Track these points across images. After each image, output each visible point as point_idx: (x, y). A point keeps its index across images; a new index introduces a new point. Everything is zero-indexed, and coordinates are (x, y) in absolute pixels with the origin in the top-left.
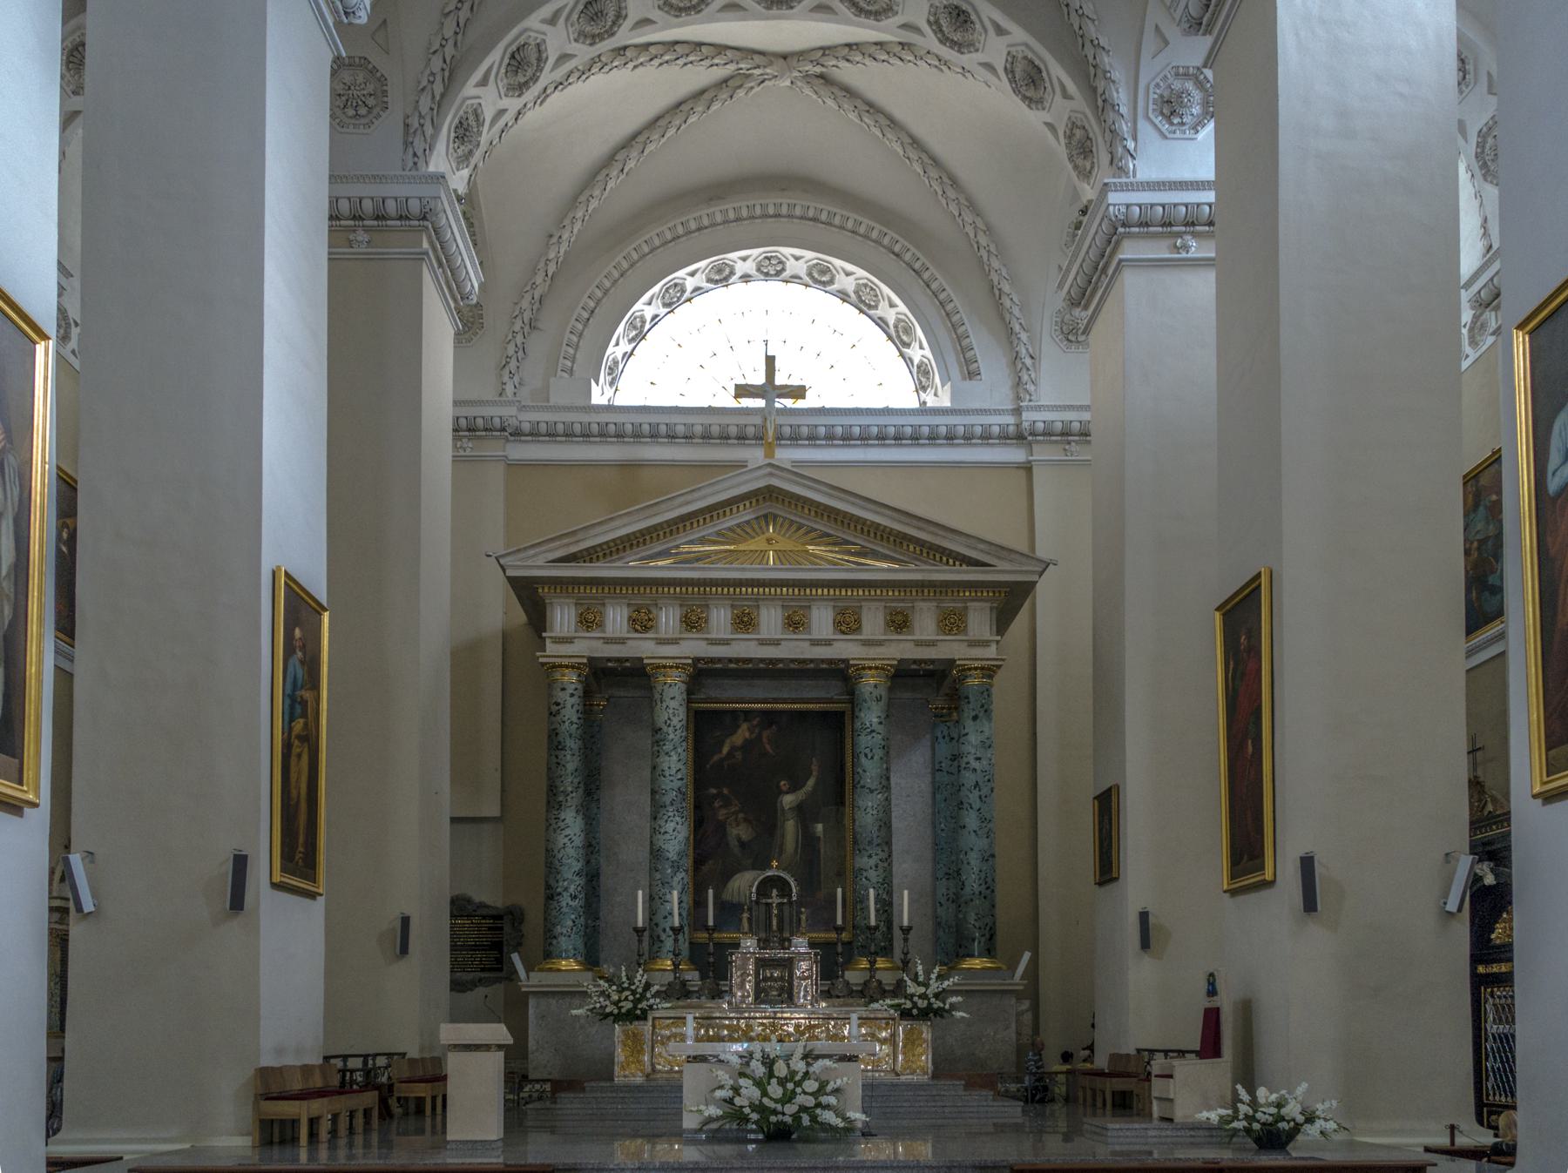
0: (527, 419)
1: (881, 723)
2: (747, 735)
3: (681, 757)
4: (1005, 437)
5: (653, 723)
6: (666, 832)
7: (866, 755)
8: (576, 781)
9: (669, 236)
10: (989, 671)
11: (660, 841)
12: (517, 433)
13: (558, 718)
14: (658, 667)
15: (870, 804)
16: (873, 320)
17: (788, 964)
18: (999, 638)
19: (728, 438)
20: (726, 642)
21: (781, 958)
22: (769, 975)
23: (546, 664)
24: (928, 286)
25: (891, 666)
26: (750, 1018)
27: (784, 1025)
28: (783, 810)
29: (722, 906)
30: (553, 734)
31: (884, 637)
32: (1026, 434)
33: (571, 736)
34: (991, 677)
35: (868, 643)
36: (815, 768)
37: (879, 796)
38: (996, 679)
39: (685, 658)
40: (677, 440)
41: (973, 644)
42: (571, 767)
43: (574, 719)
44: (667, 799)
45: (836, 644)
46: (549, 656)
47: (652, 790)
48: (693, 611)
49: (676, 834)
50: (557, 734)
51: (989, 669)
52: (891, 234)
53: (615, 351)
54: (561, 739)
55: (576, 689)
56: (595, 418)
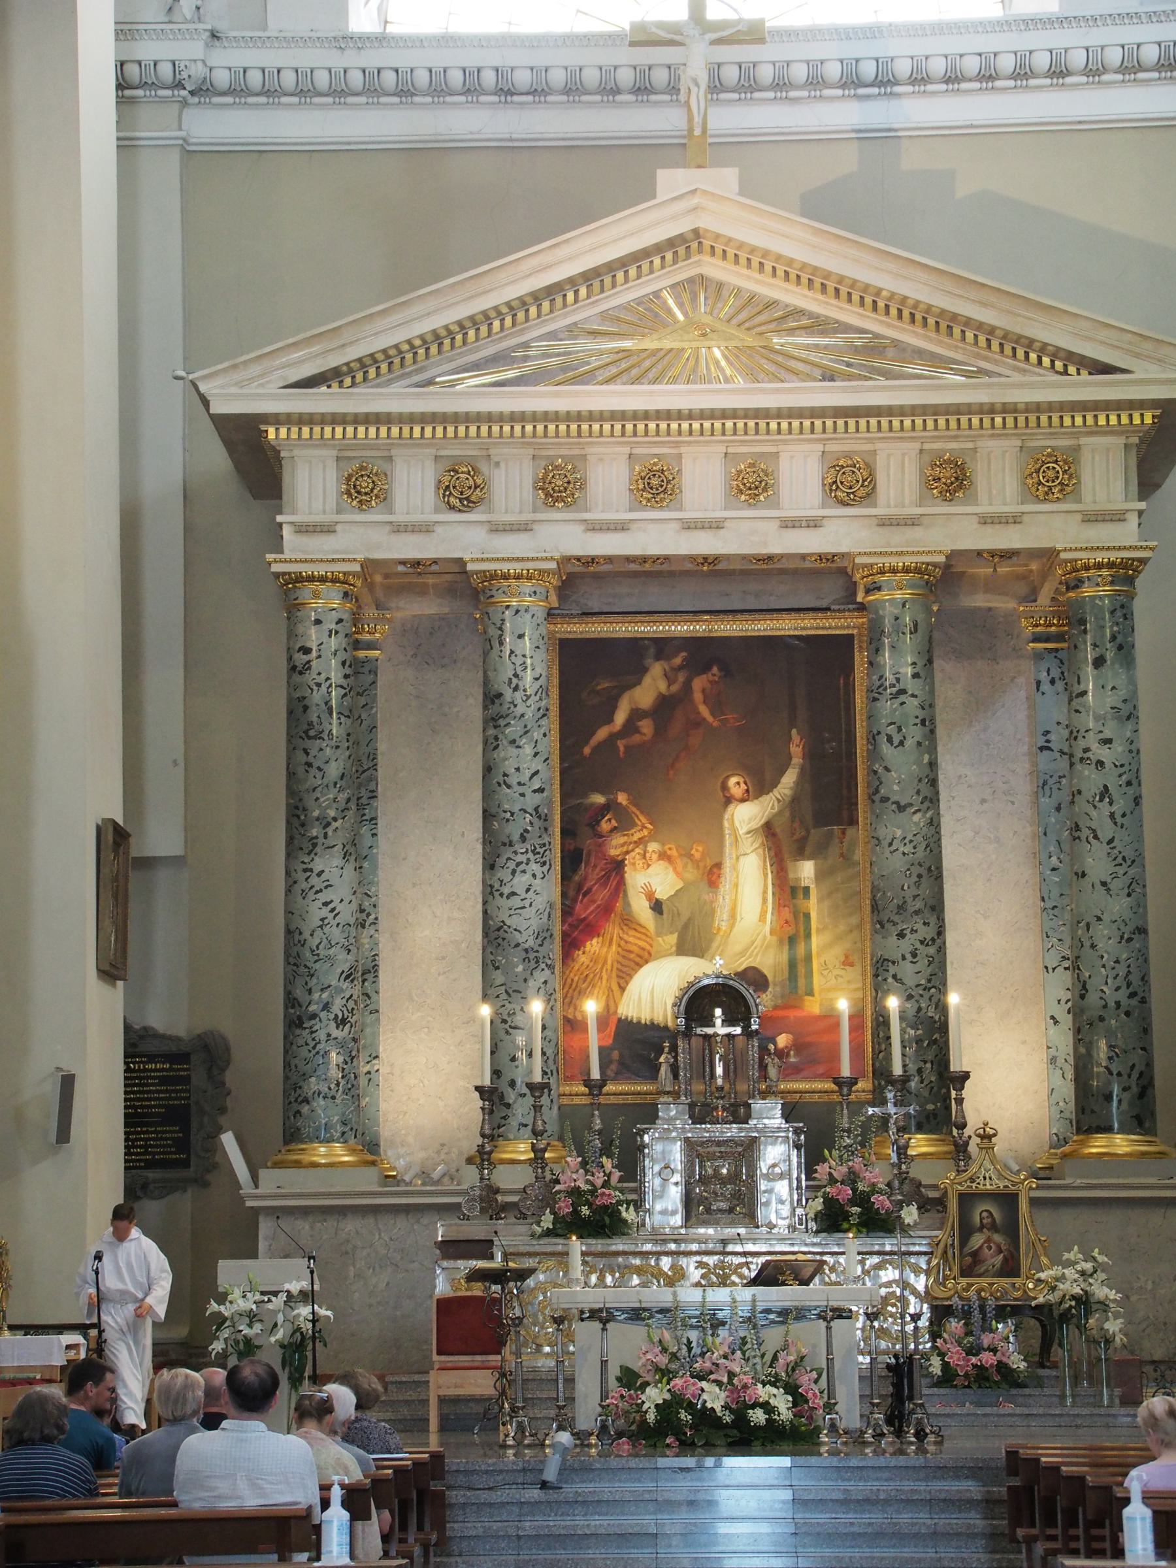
1: (915, 676)
2: (662, 686)
3: (540, 748)
6: (514, 894)
7: (890, 739)
8: (342, 797)
11: (503, 910)
12: (204, 90)
14: (493, 576)
15: (899, 833)
17: (748, 1150)
18: (1142, 505)
19: (616, 91)
20: (621, 527)
22: (710, 1171)
23: (284, 574)
25: (935, 565)
27: (740, 1266)
28: (734, 830)
31: (919, 511)
34: (1130, 581)
35: (885, 522)
37: (916, 818)
39: (546, 559)
40: (516, 98)
41: (1093, 518)
42: (334, 770)
45: (830, 527)
46: (291, 561)
47: (485, 811)
48: (557, 467)
50: (306, 708)
51: (1125, 564)
55: (340, 621)
56: (353, 60)
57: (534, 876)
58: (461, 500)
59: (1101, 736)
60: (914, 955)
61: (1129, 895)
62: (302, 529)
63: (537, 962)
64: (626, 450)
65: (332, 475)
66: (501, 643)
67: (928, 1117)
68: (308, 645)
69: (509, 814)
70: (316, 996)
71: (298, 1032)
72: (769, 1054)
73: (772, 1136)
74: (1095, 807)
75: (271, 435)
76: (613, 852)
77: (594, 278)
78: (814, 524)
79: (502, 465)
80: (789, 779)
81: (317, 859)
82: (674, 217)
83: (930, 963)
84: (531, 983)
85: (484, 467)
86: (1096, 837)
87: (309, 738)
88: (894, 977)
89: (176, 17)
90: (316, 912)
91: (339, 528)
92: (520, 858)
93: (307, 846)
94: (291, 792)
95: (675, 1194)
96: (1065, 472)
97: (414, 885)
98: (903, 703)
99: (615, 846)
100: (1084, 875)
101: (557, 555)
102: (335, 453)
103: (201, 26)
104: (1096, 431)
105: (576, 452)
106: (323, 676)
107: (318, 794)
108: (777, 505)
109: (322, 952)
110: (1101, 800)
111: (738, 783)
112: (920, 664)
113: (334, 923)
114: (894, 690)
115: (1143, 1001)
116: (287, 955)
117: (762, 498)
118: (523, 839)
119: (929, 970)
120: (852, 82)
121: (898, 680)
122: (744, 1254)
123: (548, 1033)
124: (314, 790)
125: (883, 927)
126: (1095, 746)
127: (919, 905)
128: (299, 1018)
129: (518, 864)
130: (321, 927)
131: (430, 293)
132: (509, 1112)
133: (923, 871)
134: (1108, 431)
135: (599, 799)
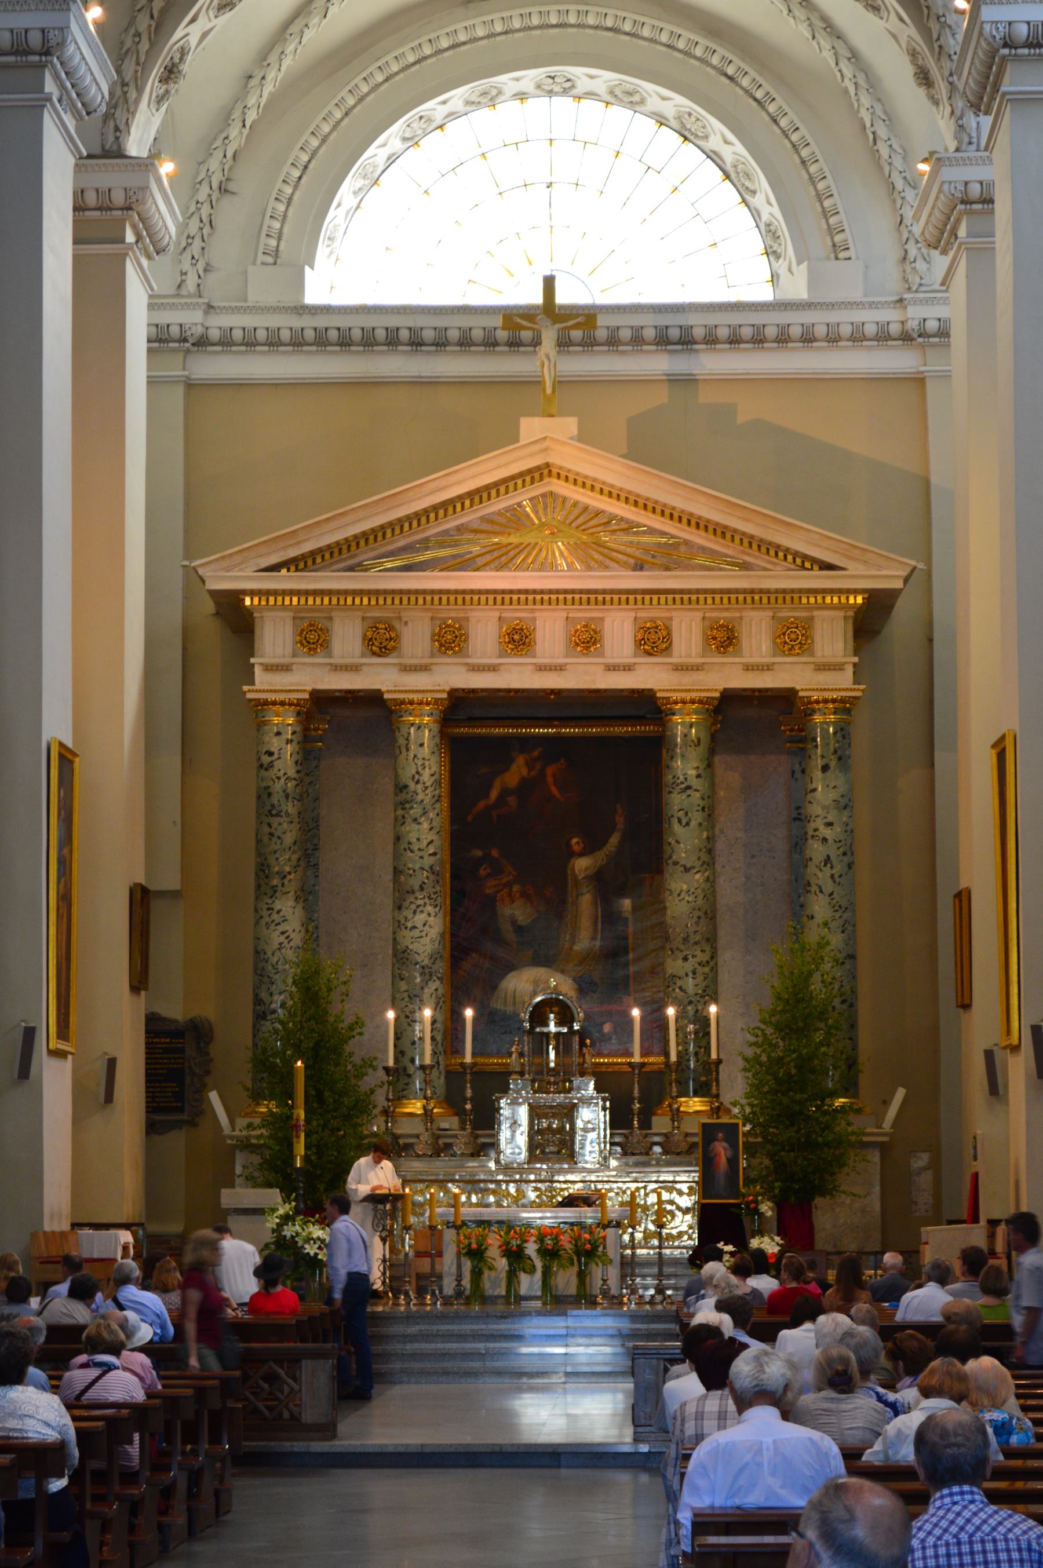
0: (218, 323)
1: (698, 776)
2: (524, 771)
3: (434, 824)
4: (883, 337)
5: (396, 776)
6: (414, 927)
7: (680, 821)
8: (295, 857)
11: (406, 938)
13: (272, 773)
14: (403, 702)
15: (685, 887)
16: (704, 152)
17: (569, 1112)
20: (493, 668)
21: (559, 1105)
23: (254, 700)
24: (775, 121)
25: (713, 698)
26: (521, 1181)
28: (575, 877)
29: (487, 1018)
30: (264, 794)
31: (703, 660)
32: (915, 335)
33: (287, 796)
34: (848, 711)
35: (679, 668)
36: (620, 821)
37: (697, 876)
40: (424, 348)
41: (821, 667)
42: (289, 839)
43: (292, 772)
46: (260, 691)
47: (395, 868)
48: (448, 626)
50: (270, 795)
52: (721, 51)
54: (274, 800)
57: (429, 915)
58: (380, 648)
59: (826, 820)
60: (694, 973)
61: (843, 932)
62: (269, 668)
63: (431, 975)
64: (497, 614)
65: (289, 629)
66: (407, 750)
67: (701, 1086)
68: (272, 749)
69: (411, 872)
70: (275, 997)
71: (263, 1022)
72: (586, 1046)
73: (587, 1102)
74: (821, 870)
75: (248, 602)
76: (488, 891)
77: (477, 495)
78: (628, 668)
79: (410, 624)
80: (614, 840)
81: (277, 901)
82: (531, 455)
83: (705, 978)
84: (426, 990)
85: (397, 625)
86: (821, 891)
87: (272, 816)
88: (680, 988)
89: (183, 292)
90: (276, 939)
91: (294, 667)
92: (419, 902)
93: (270, 892)
94: (259, 854)
95: (522, 1140)
96: (803, 635)
97: (345, 912)
98: (689, 796)
99: (490, 887)
100: (812, 917)
101: (447, 689)
102: (292, 614)
103: (200, 300)
105: (462, 615)
106: (282, 772)
107: (277, 855)
108: (602, 654)
109: (280, 967)
110: (825, 865)
111: (578, 843)
112: (702, 767)
113: (288, 946)
114: (683, 786)
115: (851, 1005)
116: (256, 969)
117: (592, 649)
118: (422, 889)
119: (705, 983)
120: (663, 340)
121: (686, 779)
122: (565, 1182)
123: (436, 1025)
124: (275, 852)
125: (673, 952)
126: (821, 828)
127: (698, 938)
128: (264, 1013)
129: (418, 906)
130: (279, 949)
131: (360, 507)
132: (410, 1080)
133: (701, 914)
134: (832, 607)
135: (479, 853)
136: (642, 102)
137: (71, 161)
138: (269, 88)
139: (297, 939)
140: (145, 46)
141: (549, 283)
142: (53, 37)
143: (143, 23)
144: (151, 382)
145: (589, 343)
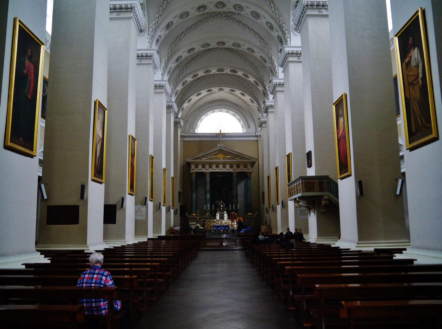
0: (187, 135)
4: (254, 136)
9: (206, 108)
10: (251, 173)
12: (185, 137)
17: (223, 215)
20: (215, 170)
35: (234, 169)
38: (252, 174)
44: (207, 191)
49: (208, 196)
53: (198, 124)
56: (196, 135)
73: (225, 213)
82: (219, 148)
95: (219, 217)
104: (248, 163)
136: (229, 113)
137: (174, 118)
138: (192, 111)
139: (195, 197)
140: (180, 107)
141: (220, 130)
142: (172, 105)
143: (180, 104)
144: (181, 141)
145: (224, 137)
